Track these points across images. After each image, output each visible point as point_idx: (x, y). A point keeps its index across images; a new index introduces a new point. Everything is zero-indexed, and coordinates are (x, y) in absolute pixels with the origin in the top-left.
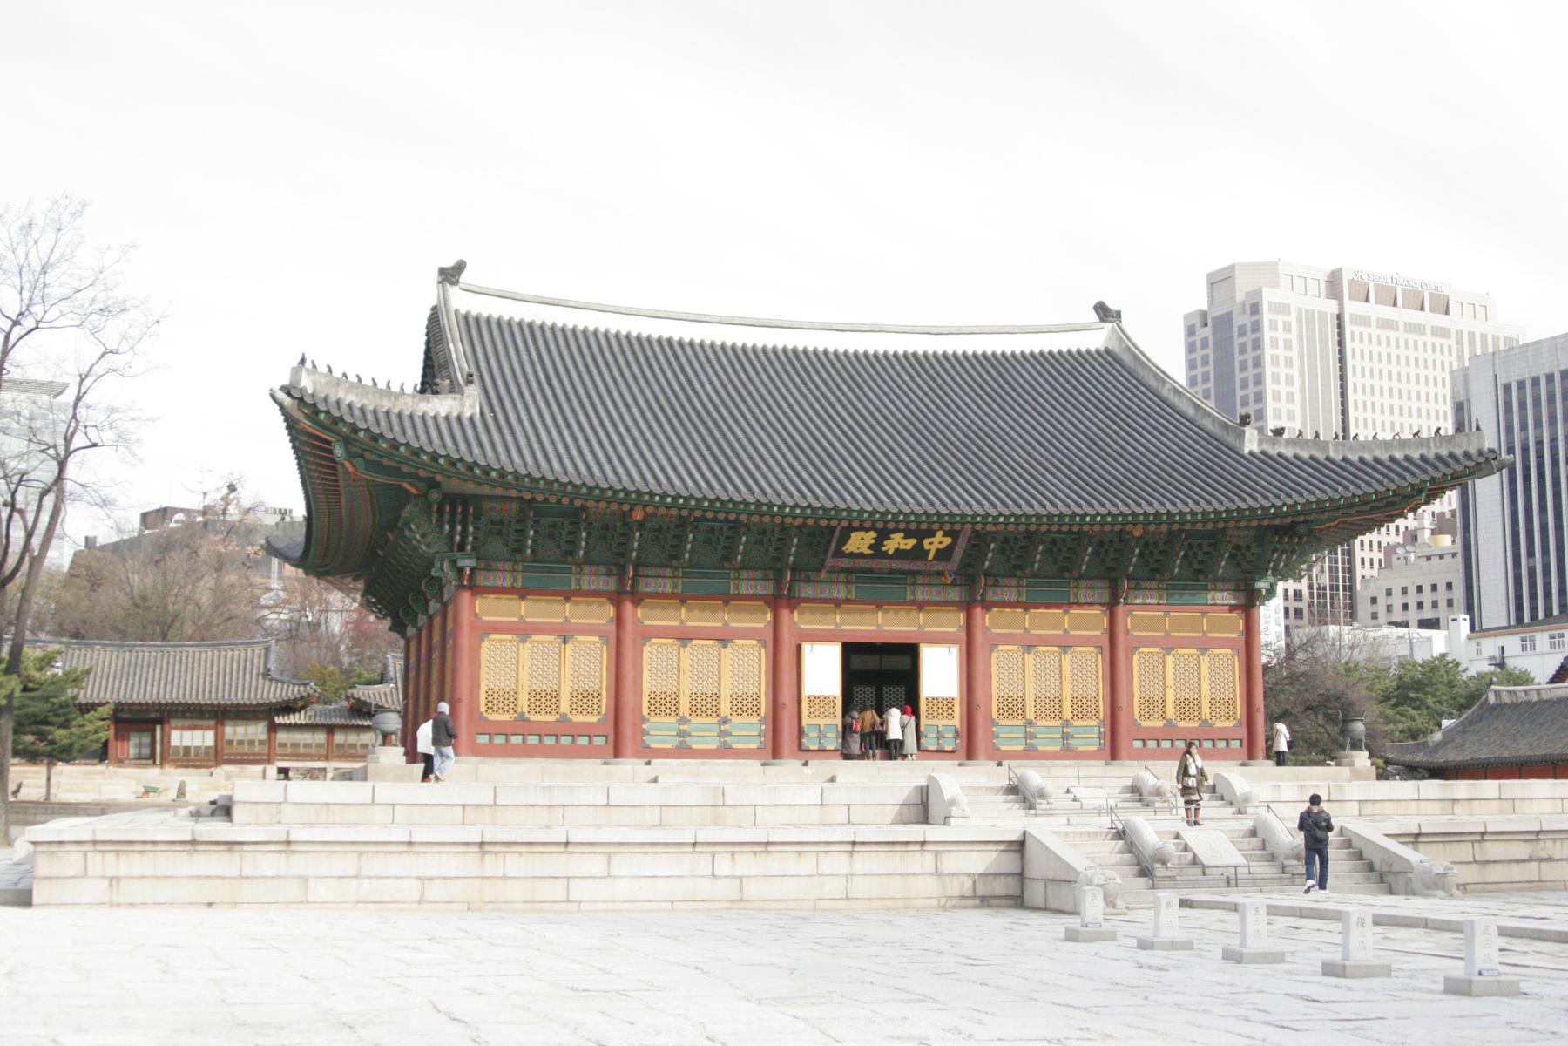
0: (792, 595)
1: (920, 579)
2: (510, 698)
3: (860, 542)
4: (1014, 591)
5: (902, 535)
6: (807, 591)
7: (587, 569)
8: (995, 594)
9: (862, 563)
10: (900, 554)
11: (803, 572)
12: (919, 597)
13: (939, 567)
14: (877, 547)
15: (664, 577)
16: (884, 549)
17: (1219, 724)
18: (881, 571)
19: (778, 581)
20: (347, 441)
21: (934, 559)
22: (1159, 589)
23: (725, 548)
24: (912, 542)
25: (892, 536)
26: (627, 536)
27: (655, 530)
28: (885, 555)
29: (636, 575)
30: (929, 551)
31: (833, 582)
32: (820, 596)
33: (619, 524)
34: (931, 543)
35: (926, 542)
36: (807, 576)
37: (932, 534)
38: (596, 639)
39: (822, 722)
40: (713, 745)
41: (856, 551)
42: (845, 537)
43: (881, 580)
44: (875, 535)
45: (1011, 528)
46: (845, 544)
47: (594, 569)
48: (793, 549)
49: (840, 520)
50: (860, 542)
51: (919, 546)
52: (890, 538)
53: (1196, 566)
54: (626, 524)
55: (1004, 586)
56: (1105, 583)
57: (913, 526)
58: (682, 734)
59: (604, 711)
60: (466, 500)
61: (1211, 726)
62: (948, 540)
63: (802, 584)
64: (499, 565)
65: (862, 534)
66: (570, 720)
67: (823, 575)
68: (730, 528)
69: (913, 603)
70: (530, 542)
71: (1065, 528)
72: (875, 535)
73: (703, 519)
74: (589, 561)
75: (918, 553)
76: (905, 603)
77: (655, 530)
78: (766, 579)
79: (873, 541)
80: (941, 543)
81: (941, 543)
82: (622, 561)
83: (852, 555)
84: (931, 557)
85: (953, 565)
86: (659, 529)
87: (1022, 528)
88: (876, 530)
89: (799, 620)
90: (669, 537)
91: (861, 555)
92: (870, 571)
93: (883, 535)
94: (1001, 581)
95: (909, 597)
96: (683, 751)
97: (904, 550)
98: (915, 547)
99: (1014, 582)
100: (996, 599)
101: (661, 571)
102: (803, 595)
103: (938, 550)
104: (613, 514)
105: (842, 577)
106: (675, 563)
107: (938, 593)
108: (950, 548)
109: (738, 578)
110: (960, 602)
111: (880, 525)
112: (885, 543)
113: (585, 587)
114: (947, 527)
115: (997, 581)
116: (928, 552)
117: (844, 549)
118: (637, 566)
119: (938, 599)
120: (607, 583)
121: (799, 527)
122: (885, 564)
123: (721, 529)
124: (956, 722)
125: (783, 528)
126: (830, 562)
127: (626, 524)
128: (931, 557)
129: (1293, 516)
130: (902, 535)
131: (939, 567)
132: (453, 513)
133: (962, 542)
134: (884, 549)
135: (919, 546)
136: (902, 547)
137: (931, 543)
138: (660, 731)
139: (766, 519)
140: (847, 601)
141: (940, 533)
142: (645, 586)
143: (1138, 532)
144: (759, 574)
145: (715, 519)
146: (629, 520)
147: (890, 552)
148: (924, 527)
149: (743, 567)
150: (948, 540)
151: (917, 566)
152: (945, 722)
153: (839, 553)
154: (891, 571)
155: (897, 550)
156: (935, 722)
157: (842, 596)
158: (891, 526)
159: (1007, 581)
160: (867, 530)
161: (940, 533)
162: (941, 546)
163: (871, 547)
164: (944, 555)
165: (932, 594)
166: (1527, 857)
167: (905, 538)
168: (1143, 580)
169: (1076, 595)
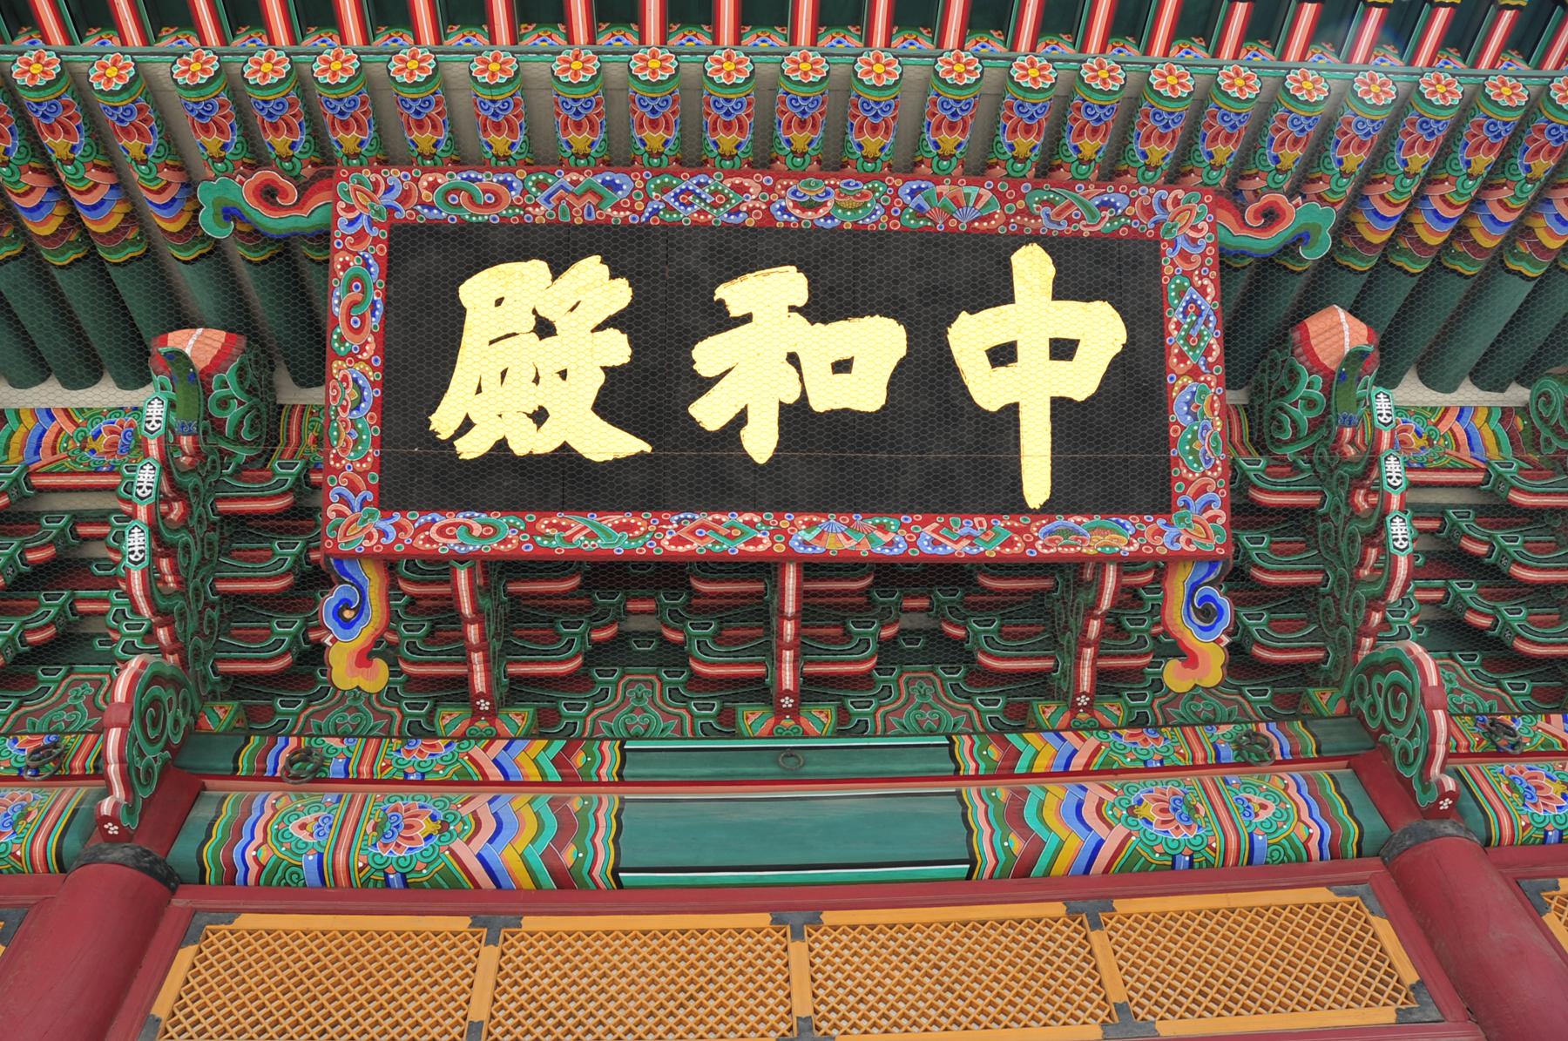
0: (182, 851)
5: (790, 284)
25: (734, 294)
30: (1011, 412)
32: (395, 856)
34: (1003, 355)
41: (528, 442)
44: (620, 294)
52: (721, 320)
72: (620, 294)
79: (617, 349)
80: (1063, 349)
81: (1063, 349)
84: (1037, 485)
97: (843, 419)
98: (900, 378)
103: (1060, 406)
116: (1011, 412)
119: (1180, 837)
130: (790, 284)
134: (710, 413)
136: (827, 396)
137: (1003, 355)
155: (795, 416)
167: (819, 310)
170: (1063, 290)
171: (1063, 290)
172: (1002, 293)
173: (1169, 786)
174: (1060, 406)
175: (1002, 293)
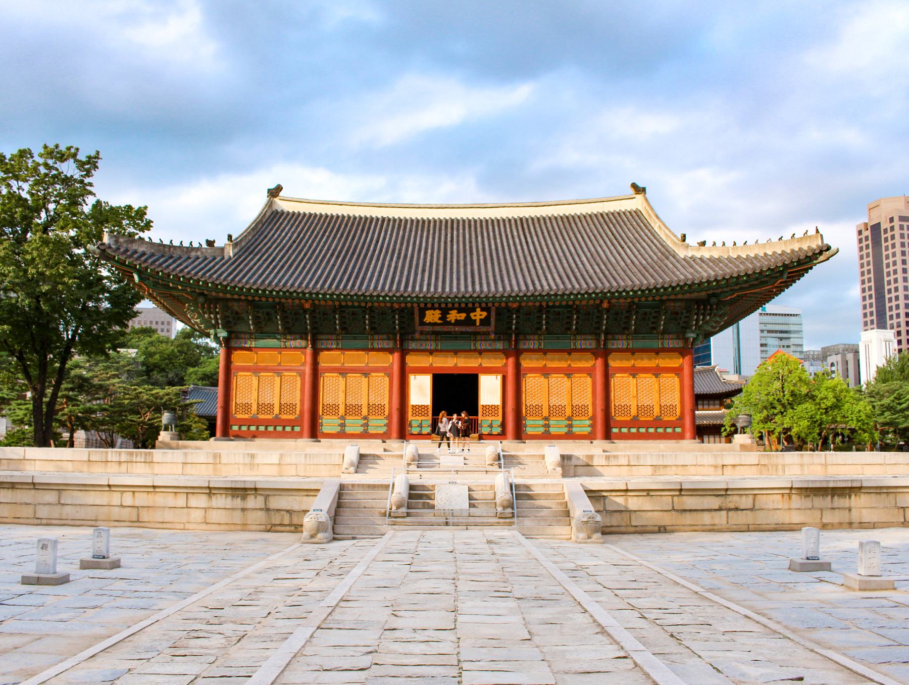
1: (479, 337)
2: (247, 407)
3: (432, 316)
4: (537, 342)
5: (456, 311)
6: (413, 345)
7: (578, 337)
8: (525, 344)
9: (438, 329)
10: (458, 323)
11: (521, 334)
12: (479, 347)
13: (484, 329)
14: (443, 317)
15: (332, 340)
16: (448, 320)
17: (666, 419)
18: (456, 333)
19: (598, 341)
20: (140, 273)
21: (480, 325)
22: (627, 339)
23: (597, 323)
24: (463, 316)
26: (600, 318)
27: (586, 314)
28: (449, 323)
29: (605, 340)
30: (475, 320)
31: (427, 340)
32: (422, 348)
33: (595, 311)
35: (472, 315)
36: (412, 337)
37: (475, 311)
38: (295, 374)
39: (420, 418)
40: (360, 430)
42: (422, 315)
43: (456, 339)
45: (530, 304)
46: (424, 318)
47: (381, 336)
48: (514, 321)
49: (366, 303)
50: (432, 316)
51: (468, 317)
53: (682, 325)
54: (599, 311)
55: (530, 340)
56: (593, 337)
57: (463, 305)
58: (343, 425)
59: (298, 412)
60: (218, 300)
61: (661, 420)
62: (485, 314)
63: (410, 342)
64: (243, 336)
65: (432, 312)
66: (280, 418)
67: (417, 336)
68: (656, 312)
69: (475, 350)
70: (337, 322)
71: (564, 303)
73: (554, 306)
74: (579, 332)
75: (469, 322)
76: (470, 351)
77: (586, 314)
78: (389, 339)
79: (440, 316)
82: (598, 331)
83: (430, 324)
84: (478, 324)
85: (492, 328)
86: (617, 314)
87: (537, 304)
88: (440, 309)
89: (412, 361)
90: (623, 317)
91: (435, 324)
92: (449, 333)
93: (445, 312)
94: (528, 337)
95: (472, 348)
96: (342, 435)
97: (460, 320)
98: (466, 317)
99: (536, 337)
100: (237, 346)
101: (330, 337)
102: (410, 348)
103: (481, 320)
104: (592, 305)
105: (433, 337)
106: (627, 332)
107: (490, 345)
108: (487, 319)
109: (475, 340)
110: (504, 349)
111: (443, 306)
112: (448, 316)
113: (579, 347)
114: (484, 305)
115: (525, 337)
116: (475, 320)
117: (425, 320)
118: (606, 334)
119: (490, 348)
120: (590, 344)
121: (518, 310)
122: (450, 328)
123: (650, 313)
124: (500, 418)
125: (394, 311)
126: (418, 328)
127: (599, 311)
128: (478, 324)
129: (706, 291)
131: (484, 329)
132: (209, 308)
133: (493, 314)
135: (468, 317)
136: (459, 318)
138: (328, 424)
139: (382, 305)
140: (437, 351)
141: (478, 310)
142: (522, 346)
143: (515, 305)
144: (385, 337)
145: (353, 307)
146: (600, 308)
147: (453, 321)
148: (470, 305)
149: (664, 332)
150: (485, 314)
151: (470, 329)
152: (423, 418)
153: (422, 323)
154: (462, 333)
155: (456, 320)
156: (487, 418)
157: (433, 347)
158: (450, 306)
159: (532, 337)
160: (435, 309)
161: (478, 310)
162: (482, 317)
163: (440, 319)
164: (485, 322)
165: (485, 345)
166: (717, 507)
167: (458, 313)
168: (528, 334)
169: (475, 345)
170: (481, 311)
171: (481, 311)
172: (475, 311)
173: (490, 342)
174: (481, 320)
175: (475, 311)
